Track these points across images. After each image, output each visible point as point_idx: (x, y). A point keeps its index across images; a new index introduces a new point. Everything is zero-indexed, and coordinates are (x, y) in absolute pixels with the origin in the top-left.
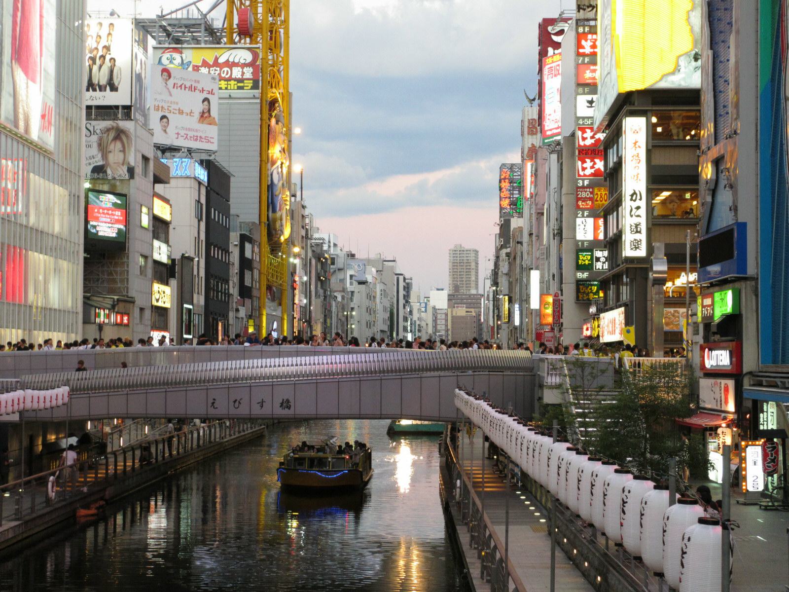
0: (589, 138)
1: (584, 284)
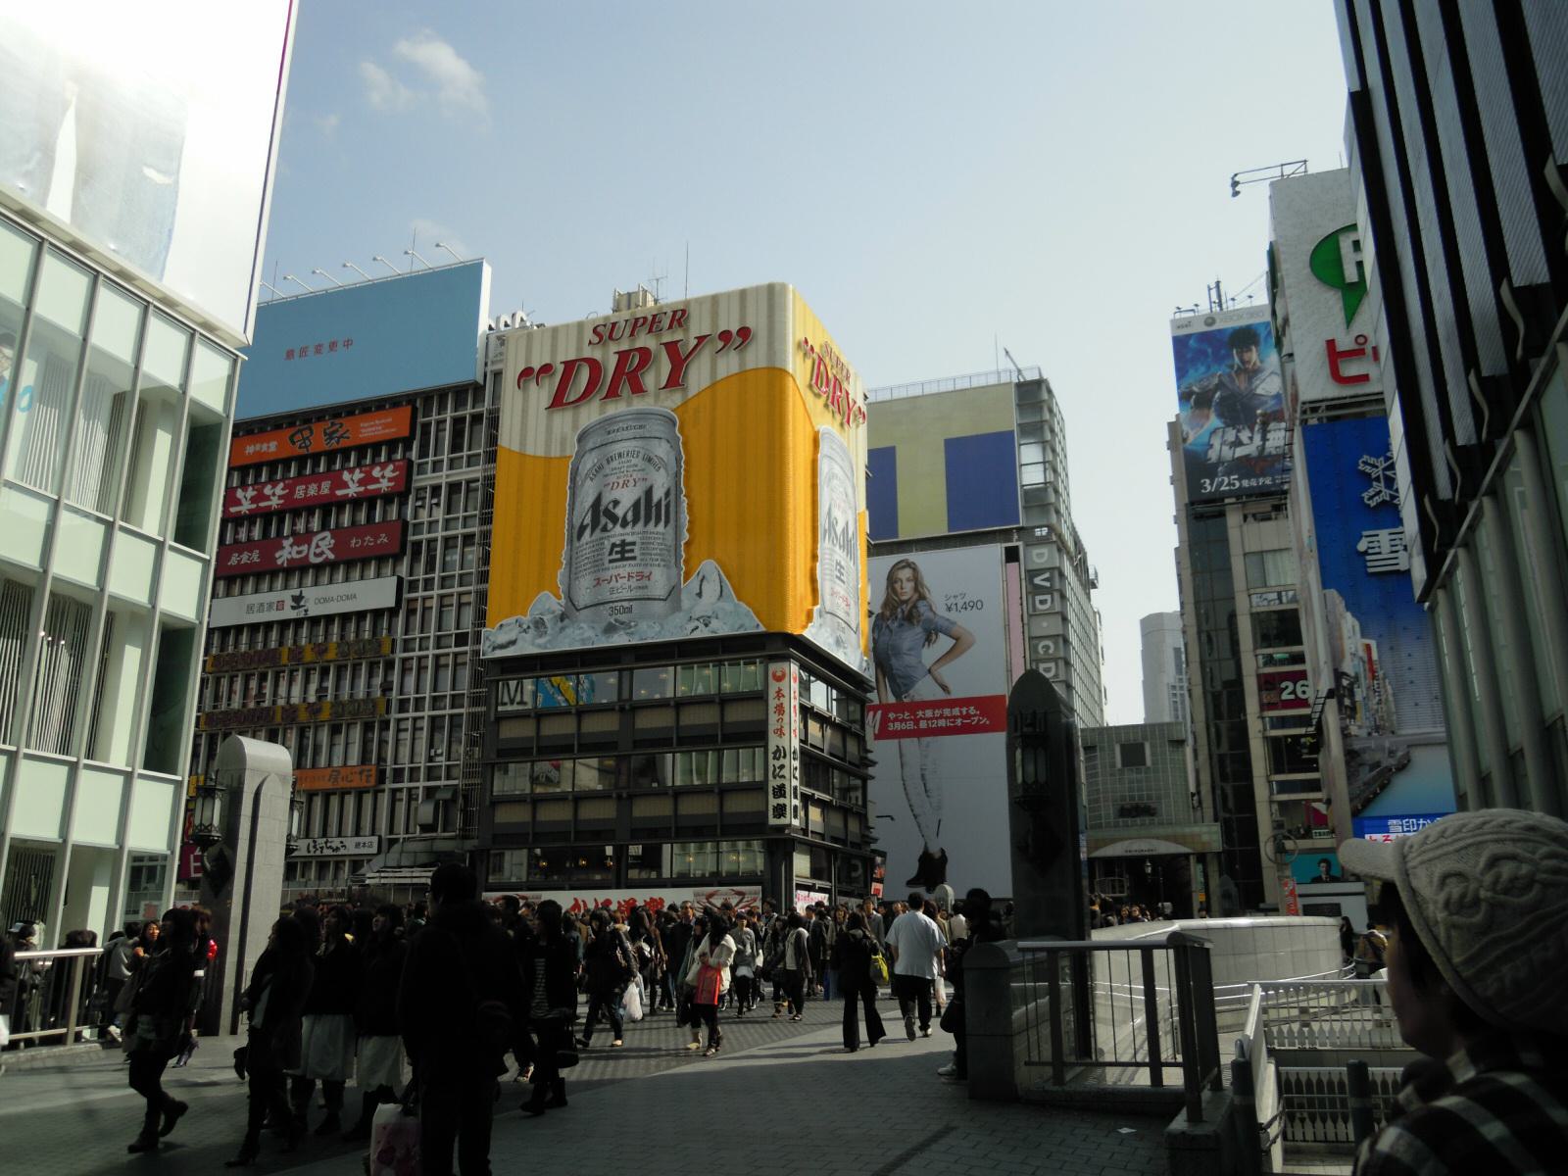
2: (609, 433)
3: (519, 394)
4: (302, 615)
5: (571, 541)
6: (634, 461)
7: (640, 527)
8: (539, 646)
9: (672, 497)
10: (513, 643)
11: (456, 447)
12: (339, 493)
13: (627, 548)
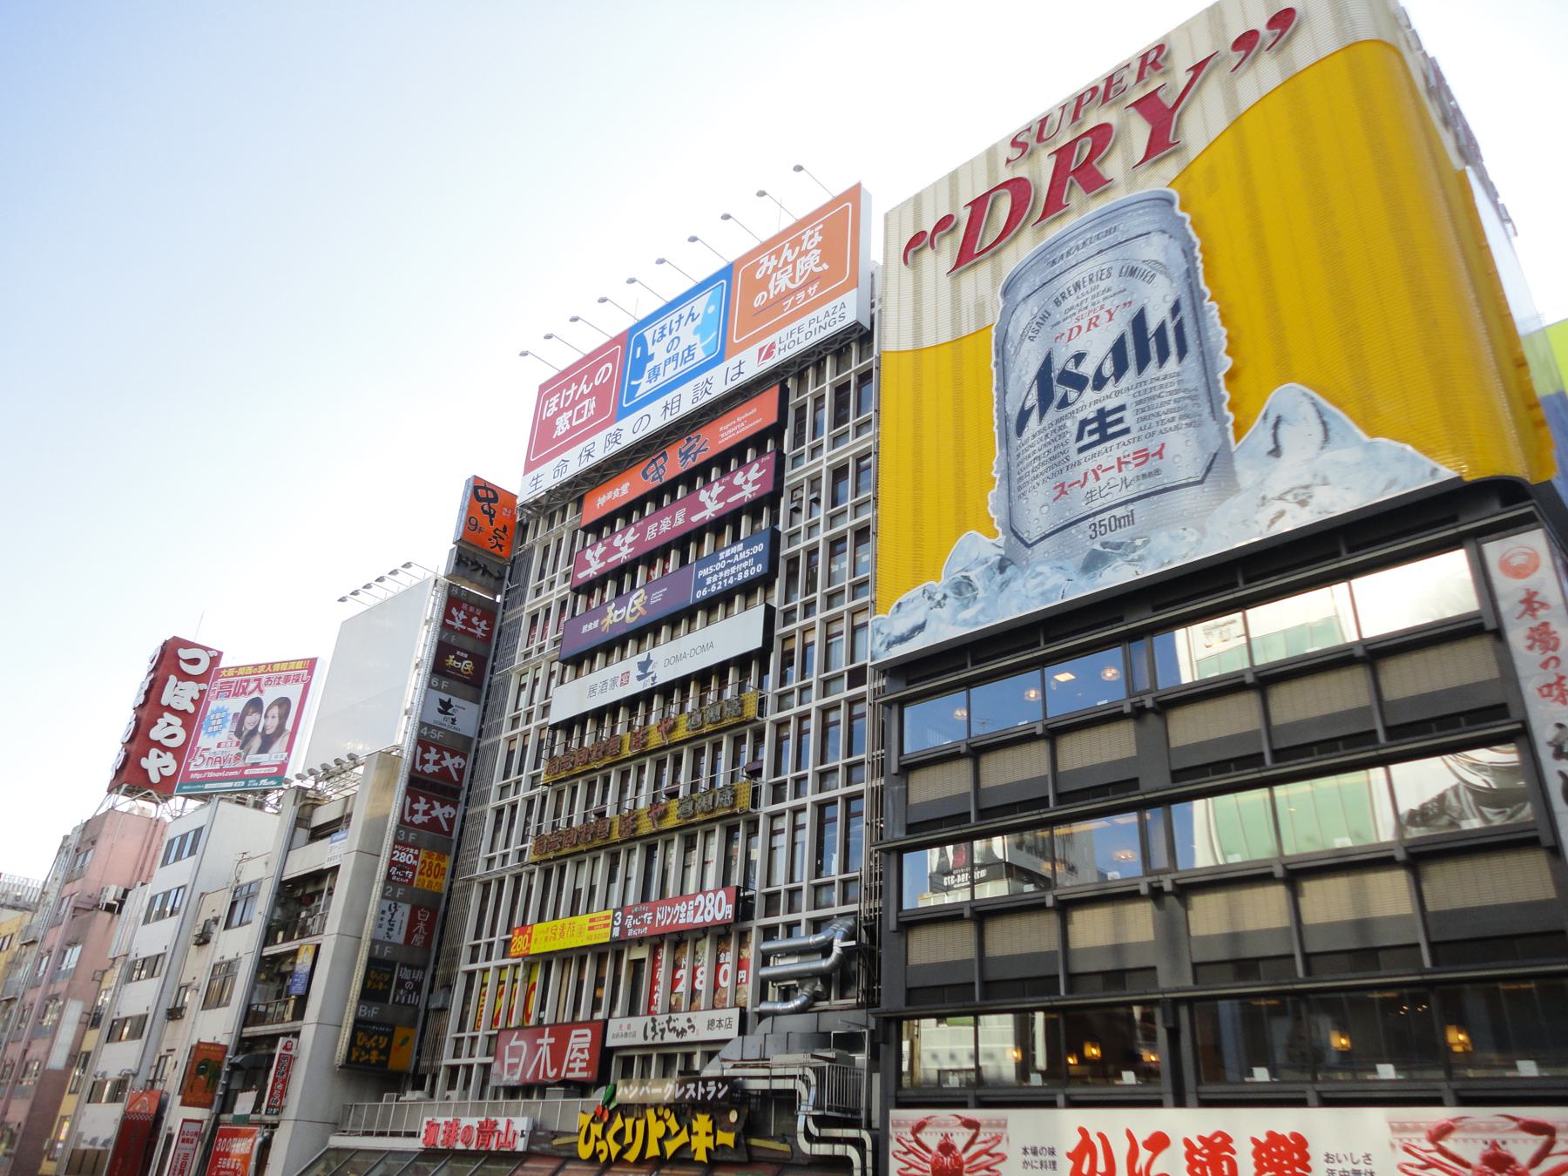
0: (431, 762)
1: (364, 1031)
2: (1054, 262)
3: (907, 273)
4: (649, 686)
5: (1006, 441)
6: (1103, 285)
7: (1130, 376)
8: (965, 623)
9: (1186, 312)
10: (920, 628)
11: (839, 418)
12: (695, 519)
13: (1109, 419)
